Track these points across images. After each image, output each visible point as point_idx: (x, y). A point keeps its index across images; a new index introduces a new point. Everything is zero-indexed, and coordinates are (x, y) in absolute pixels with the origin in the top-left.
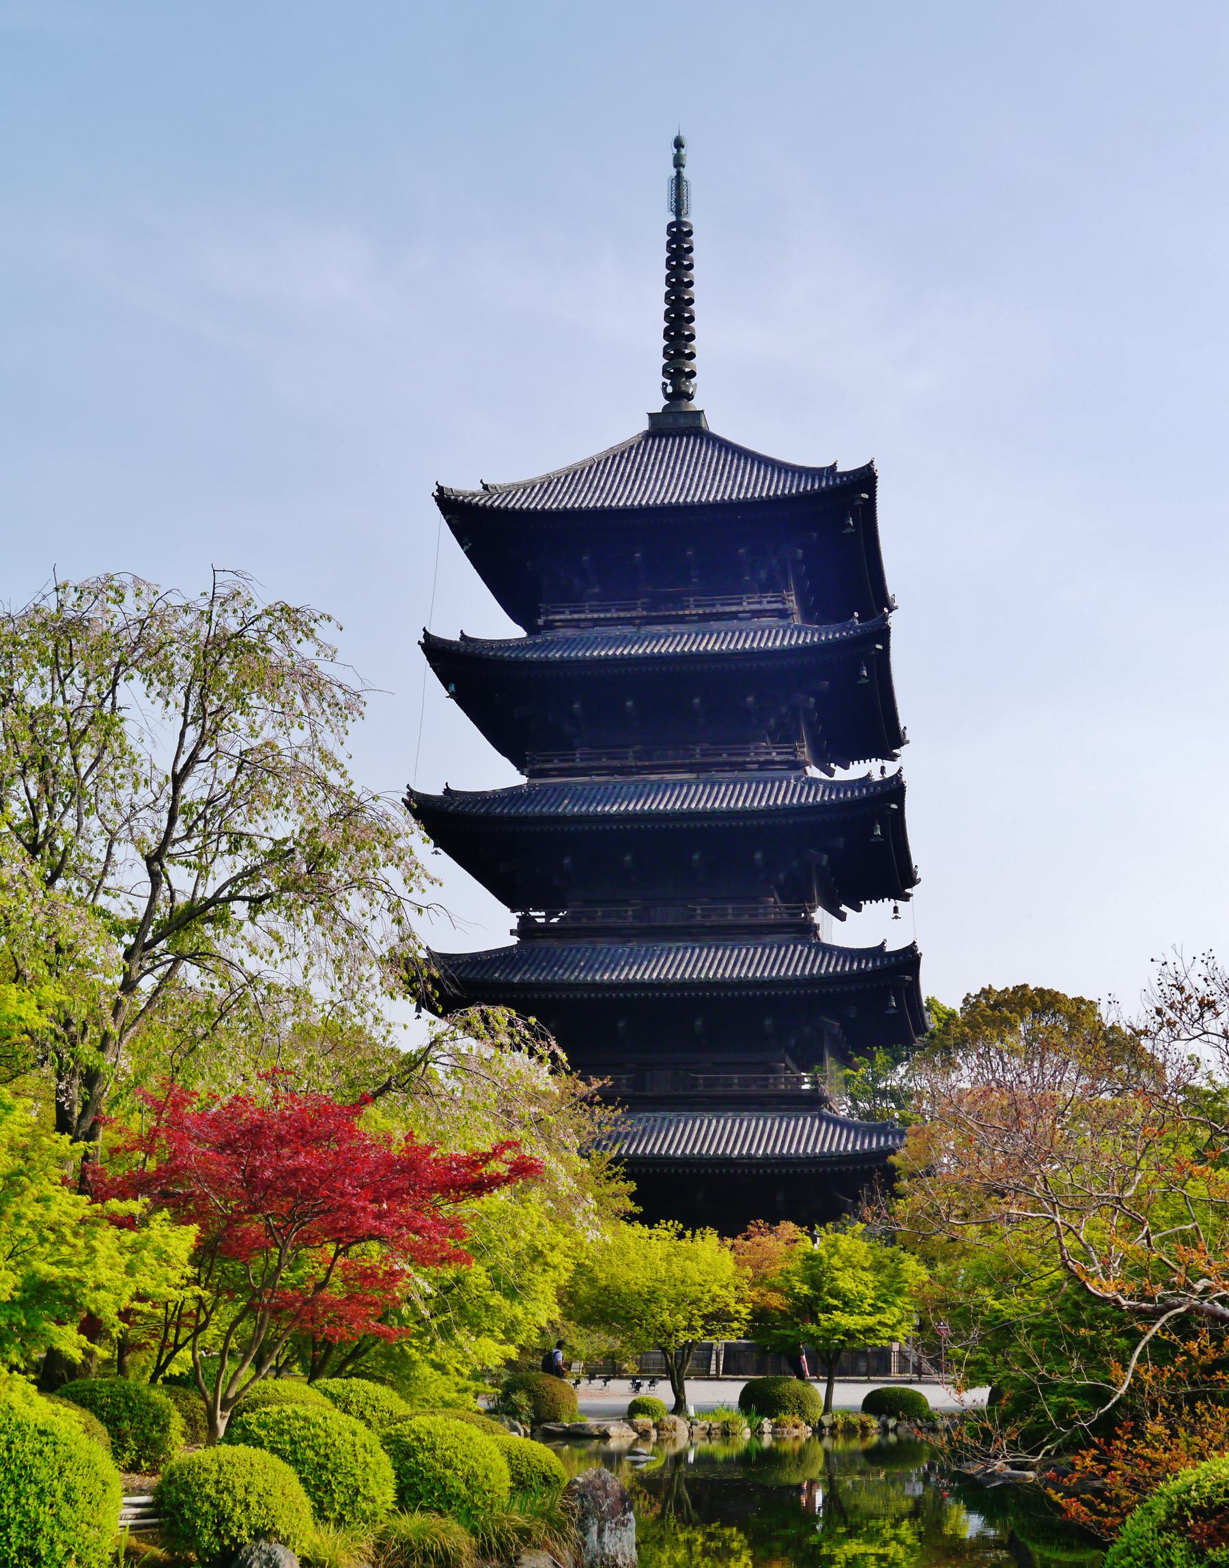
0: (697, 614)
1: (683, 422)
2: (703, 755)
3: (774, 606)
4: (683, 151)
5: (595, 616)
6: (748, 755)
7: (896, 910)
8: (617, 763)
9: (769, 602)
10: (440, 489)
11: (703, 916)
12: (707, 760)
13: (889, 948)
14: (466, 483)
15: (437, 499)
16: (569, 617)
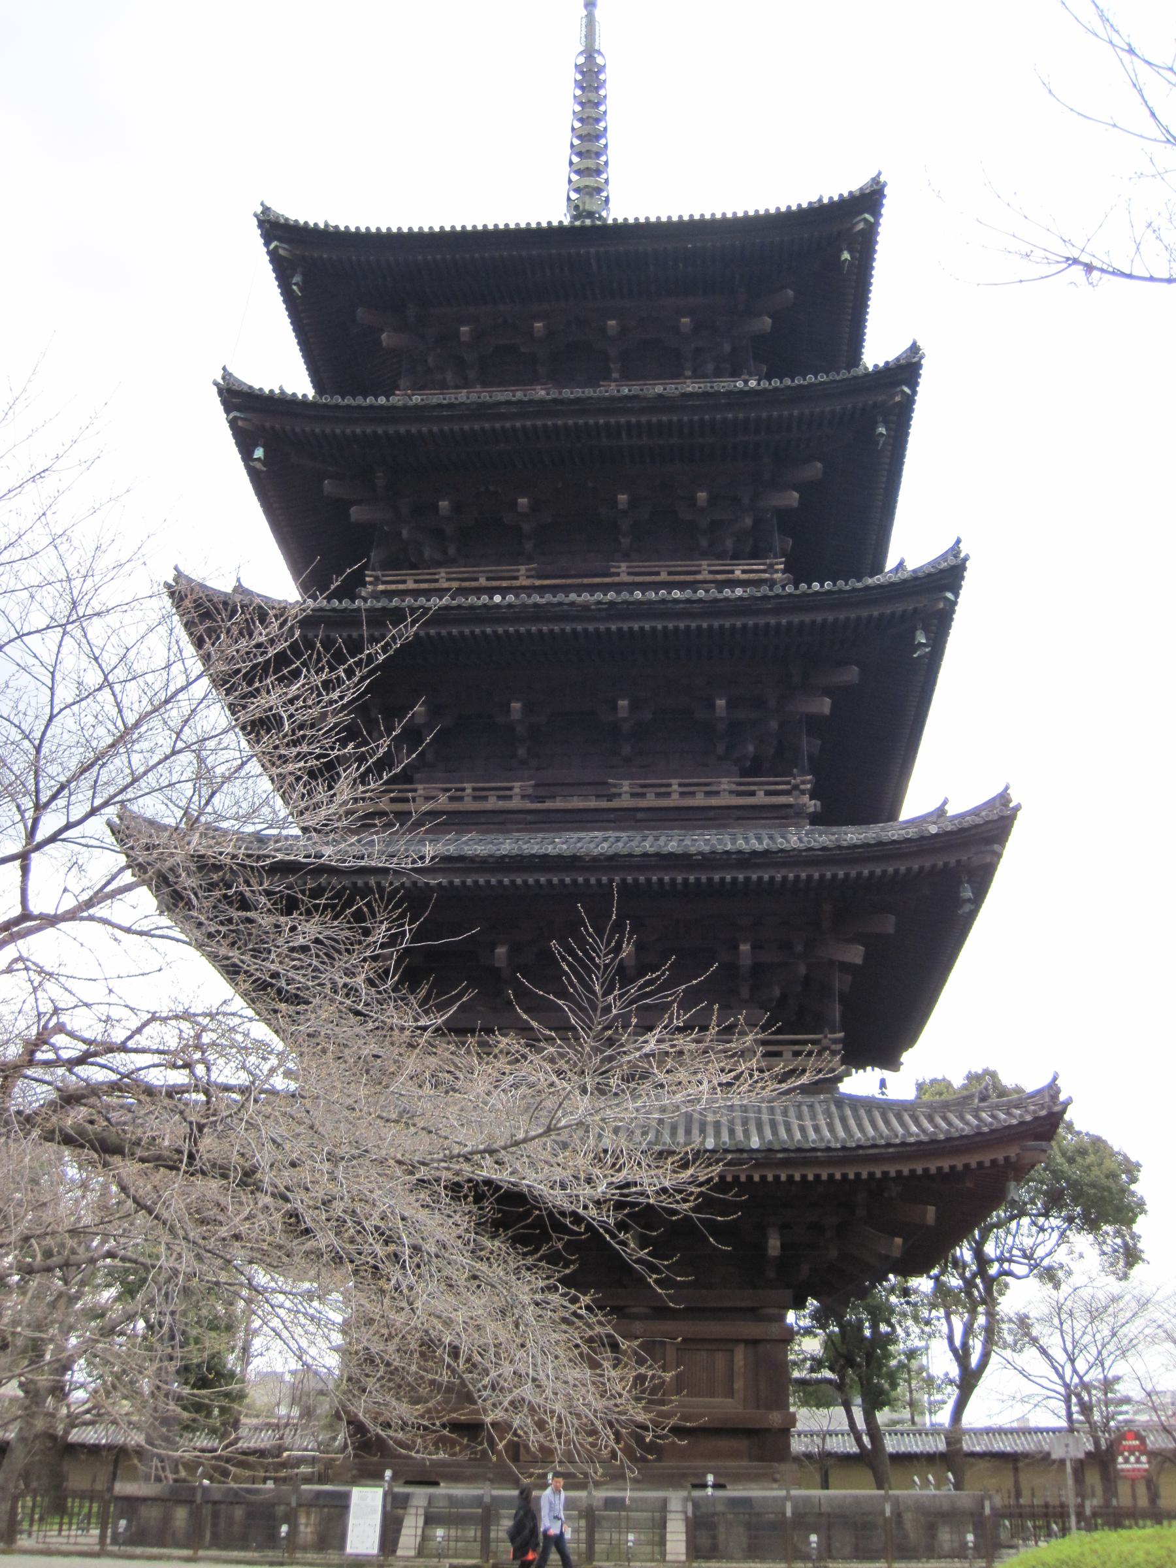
10: (266, 210)
13: (952, 810)
15: (261, 224)
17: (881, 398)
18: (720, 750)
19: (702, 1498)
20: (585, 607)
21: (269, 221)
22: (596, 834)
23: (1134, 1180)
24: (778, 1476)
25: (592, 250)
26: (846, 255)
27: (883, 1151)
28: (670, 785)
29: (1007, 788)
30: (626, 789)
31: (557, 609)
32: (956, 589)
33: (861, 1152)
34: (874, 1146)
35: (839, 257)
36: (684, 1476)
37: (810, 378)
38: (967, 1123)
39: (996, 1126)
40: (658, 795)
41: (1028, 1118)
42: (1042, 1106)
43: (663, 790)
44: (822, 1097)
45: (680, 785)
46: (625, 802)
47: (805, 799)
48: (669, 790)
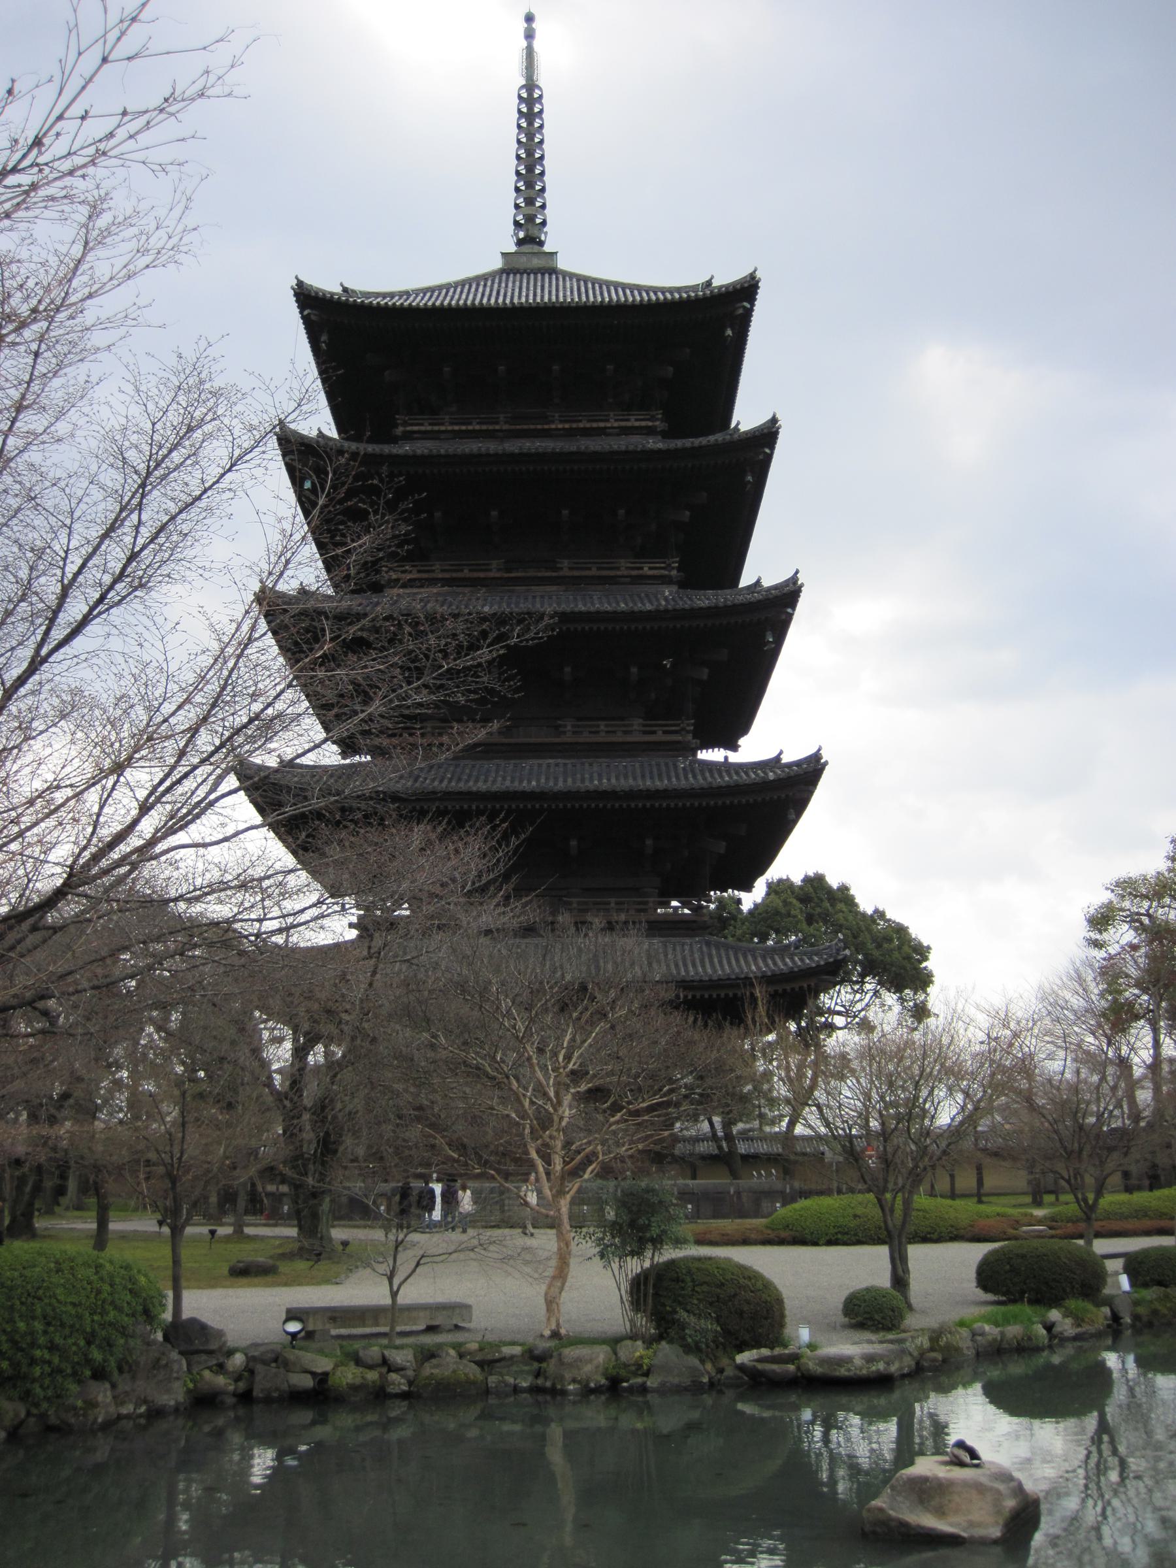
0: (564, 429)
1: (536, 262)
2: (571, 569)
3: (643, 424)
4: (534, 26)
5: (456, 428)
6: (618, 569)
8: (482, 575)
9: (637, 420)
10: (300, 284)
11: (574, 733)
12: (576, 573)
13: (786, 759)
14: (328, 283)
15: (296, 295)
16: (429, 428)
21: (303, 294)
22: (551, 761)
23: (926, 959)
26: (729, 332)
29: (819, 750)
30: (569, 728)
32: (793, 604)
34: (729, 979)
35: (724, 332)
38: (786, 964)
39: (803, 967)
41: (822, 963)
42: (831, 956)
45: (606, 726)
47: (690, 737)
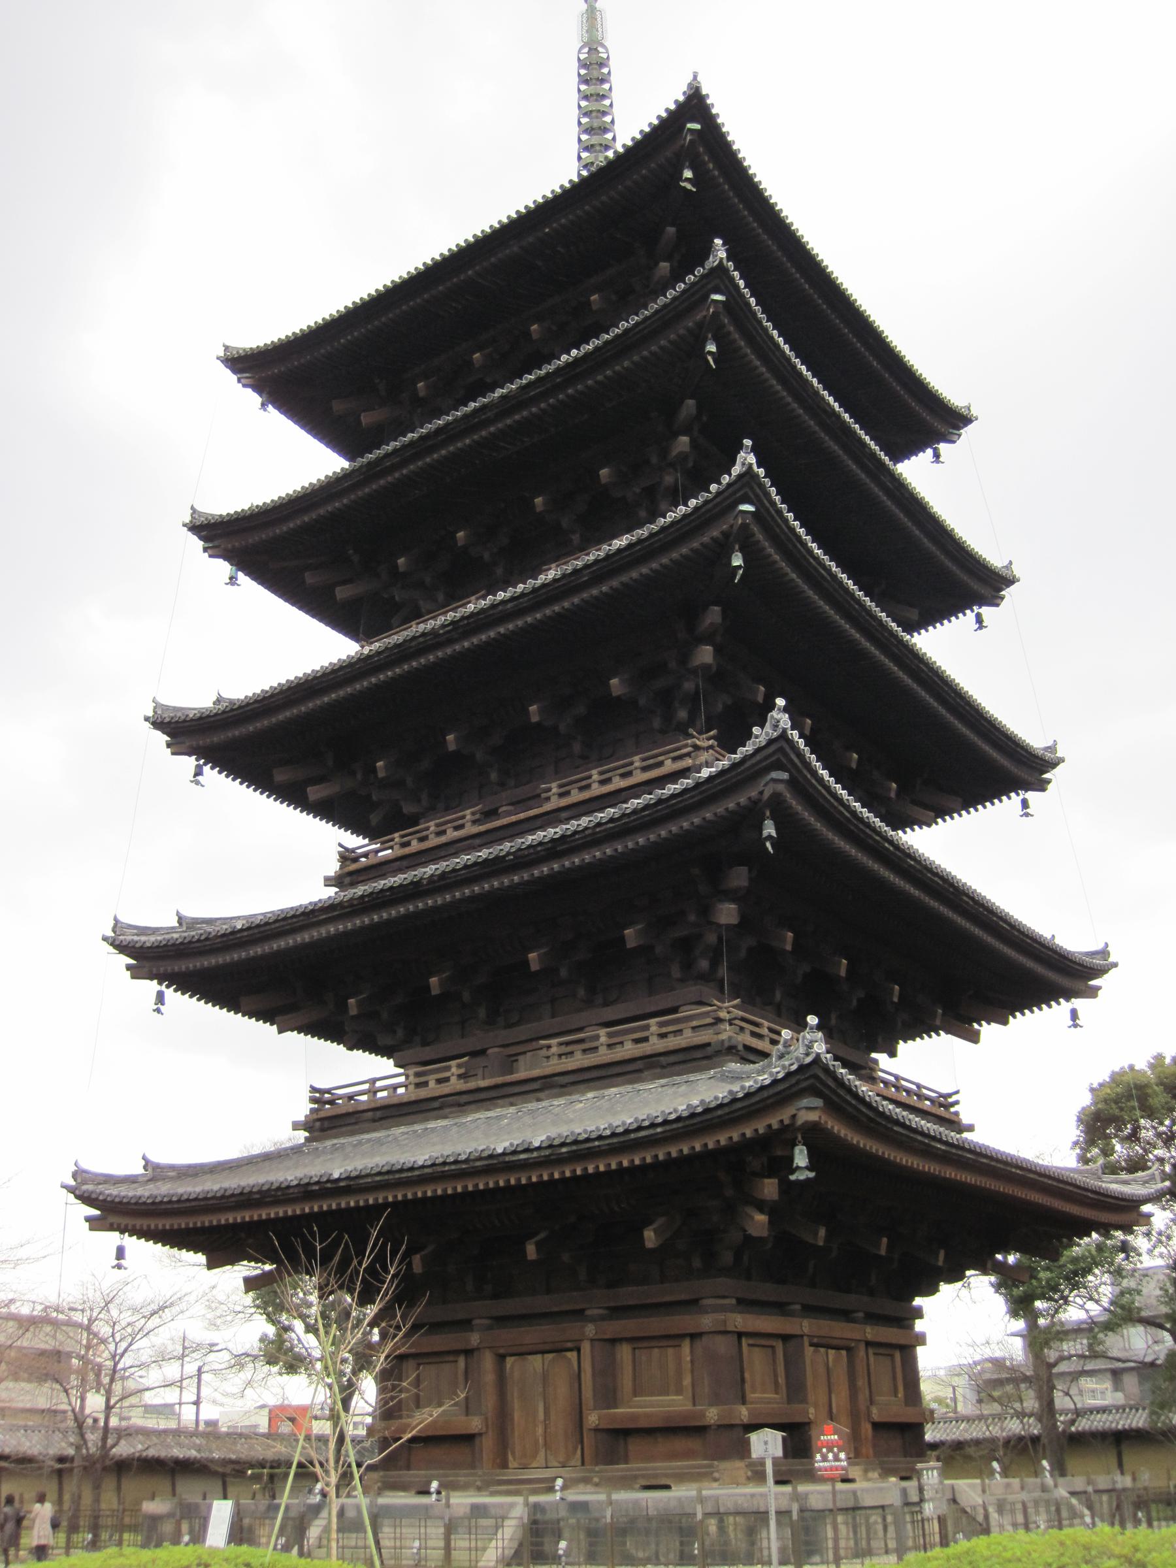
7: (1025, 804)
10: (227, 348)
17: (699, 317)
18: (657, 723)
19: (547, 1503)
20: (434, 632)
24: (716, 1475)
25: (470, 272)
27: (651, 1131)
28: (590, 777)
31: (413, 644)
33: (632, 1136)
36: (636, 1477)
37: (624, 325)
40: (581, 789)
43: (584, 783)
44: (712, 1072)
46: (554, 803)
48: (589, 781)
